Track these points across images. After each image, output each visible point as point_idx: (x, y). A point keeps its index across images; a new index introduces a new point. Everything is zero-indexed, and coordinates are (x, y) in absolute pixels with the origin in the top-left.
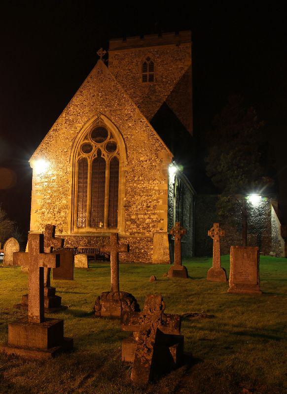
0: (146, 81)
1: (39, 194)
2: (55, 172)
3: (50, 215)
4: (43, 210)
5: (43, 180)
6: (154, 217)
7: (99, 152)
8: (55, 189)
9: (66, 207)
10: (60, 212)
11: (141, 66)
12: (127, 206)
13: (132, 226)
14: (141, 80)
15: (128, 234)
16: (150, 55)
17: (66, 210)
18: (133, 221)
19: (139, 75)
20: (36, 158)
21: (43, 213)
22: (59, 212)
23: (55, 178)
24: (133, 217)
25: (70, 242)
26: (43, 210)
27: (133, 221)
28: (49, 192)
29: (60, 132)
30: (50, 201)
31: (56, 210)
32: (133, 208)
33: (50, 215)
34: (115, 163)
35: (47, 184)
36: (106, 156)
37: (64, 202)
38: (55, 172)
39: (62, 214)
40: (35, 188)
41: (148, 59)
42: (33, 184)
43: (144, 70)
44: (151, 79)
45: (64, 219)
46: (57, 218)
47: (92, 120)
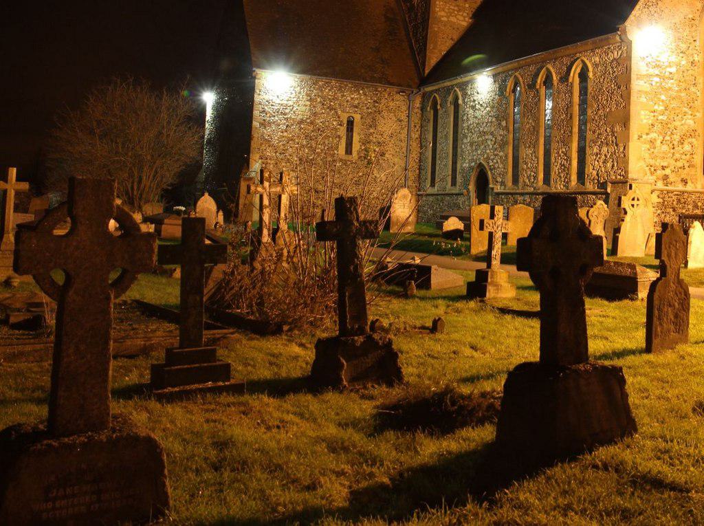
1: (643, 99)
2: (674, 58)
3: (665, 148)
4: (653, 135)
5: (652, 71)
8: (674, 94)
10: (682, 144)
17: (694, 140)
20: (639, 22)
21: (652, 142)
22: (681, 143)
23: (673, 70)
25: (700, 204)
26: (653, 135)
28: (663, 97)
31: (677, 138)
33: (665, 148)
35: (657, 79)
38: (674, 58)
39: (687, 147)
40: (637, 85)
42: (633, 76)
46: (677, 156)
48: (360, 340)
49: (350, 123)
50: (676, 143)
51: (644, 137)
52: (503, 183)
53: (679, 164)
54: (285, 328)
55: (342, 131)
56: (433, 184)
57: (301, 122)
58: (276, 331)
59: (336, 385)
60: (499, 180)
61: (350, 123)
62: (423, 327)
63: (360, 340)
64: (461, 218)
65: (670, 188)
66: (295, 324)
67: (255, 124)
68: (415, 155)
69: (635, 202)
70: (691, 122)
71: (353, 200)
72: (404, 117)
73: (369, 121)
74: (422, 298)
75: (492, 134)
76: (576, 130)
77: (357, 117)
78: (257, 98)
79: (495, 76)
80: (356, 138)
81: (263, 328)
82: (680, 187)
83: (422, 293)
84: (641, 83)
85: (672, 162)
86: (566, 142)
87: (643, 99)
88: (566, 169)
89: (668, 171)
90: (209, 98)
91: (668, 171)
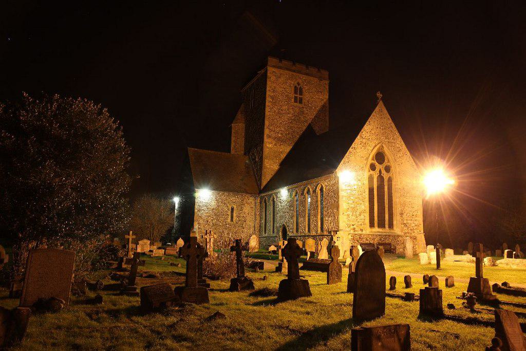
0: (297, 102)
3: (354, 217)
4: (349, 213)
6: (416, 223)
7: (380, 171)
8: (356, 196)
9: (364, 211)
11: (293, 88)
12: (402, 214)
13: (405, 229)
14: (293, 100)
15: (403, 234)
16: (300, 81)
18: (405, 225)
19: (292, 95)
20: (341, 169)
21: (348, 215)
22: (360, 215)
23: (356, 187)
24: (405, 222)
26: (349, 213)
27: (405, 225)
29: (358, 150)
30: (353, 206)
31: (358, 213)
32: (404, 216)
33: (354, 217)
34: (390, 180)
35: (349, 191)
36: (386, 176)
37: (363, 207)
38: (356, 183)
40: (341, 194)
41: (299, 84)
42: (340, 191)
43: (296, 92)
44: (301, 102)
45: (363, 220)
47: (378, 147)
48: (243, 278)
49: (232, 209)
50: (358, 215)
51: (345, 213)
52: (293, 232)
53: (360, 223)
54: (220, 278)
55: (229, 213)
56: (265, 233)
57: (213, 209)
58: (218, 279)
59: (237, 290)
60: (291, 231)
61: (232, 209)
62: (260, 279)
63: (243, 278)
64: (275, 246)
65: (356, 233)
66: (223, 277)
67: (196, 211)
68: (258, 221)
69: (338, 239)
70: (363, 207)
71: (240, 240)
72: (253, 205)
73: (239, 208)
74: (260, 272)
75: (288, 212)
76: (319, 211)
77: (235, 207)
78: (196, 201)
79: (288, 190)
80: (235, 215)
81: (214, 278)
82: (360, 232)
83: (261, 271)
84: (343, 192)
85: (357, 223)
86: (316, 216)
87: (344, 199)
88: (316, 226)
89: (355, 226)
90: (176, 200)
91: (355, 226)
